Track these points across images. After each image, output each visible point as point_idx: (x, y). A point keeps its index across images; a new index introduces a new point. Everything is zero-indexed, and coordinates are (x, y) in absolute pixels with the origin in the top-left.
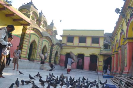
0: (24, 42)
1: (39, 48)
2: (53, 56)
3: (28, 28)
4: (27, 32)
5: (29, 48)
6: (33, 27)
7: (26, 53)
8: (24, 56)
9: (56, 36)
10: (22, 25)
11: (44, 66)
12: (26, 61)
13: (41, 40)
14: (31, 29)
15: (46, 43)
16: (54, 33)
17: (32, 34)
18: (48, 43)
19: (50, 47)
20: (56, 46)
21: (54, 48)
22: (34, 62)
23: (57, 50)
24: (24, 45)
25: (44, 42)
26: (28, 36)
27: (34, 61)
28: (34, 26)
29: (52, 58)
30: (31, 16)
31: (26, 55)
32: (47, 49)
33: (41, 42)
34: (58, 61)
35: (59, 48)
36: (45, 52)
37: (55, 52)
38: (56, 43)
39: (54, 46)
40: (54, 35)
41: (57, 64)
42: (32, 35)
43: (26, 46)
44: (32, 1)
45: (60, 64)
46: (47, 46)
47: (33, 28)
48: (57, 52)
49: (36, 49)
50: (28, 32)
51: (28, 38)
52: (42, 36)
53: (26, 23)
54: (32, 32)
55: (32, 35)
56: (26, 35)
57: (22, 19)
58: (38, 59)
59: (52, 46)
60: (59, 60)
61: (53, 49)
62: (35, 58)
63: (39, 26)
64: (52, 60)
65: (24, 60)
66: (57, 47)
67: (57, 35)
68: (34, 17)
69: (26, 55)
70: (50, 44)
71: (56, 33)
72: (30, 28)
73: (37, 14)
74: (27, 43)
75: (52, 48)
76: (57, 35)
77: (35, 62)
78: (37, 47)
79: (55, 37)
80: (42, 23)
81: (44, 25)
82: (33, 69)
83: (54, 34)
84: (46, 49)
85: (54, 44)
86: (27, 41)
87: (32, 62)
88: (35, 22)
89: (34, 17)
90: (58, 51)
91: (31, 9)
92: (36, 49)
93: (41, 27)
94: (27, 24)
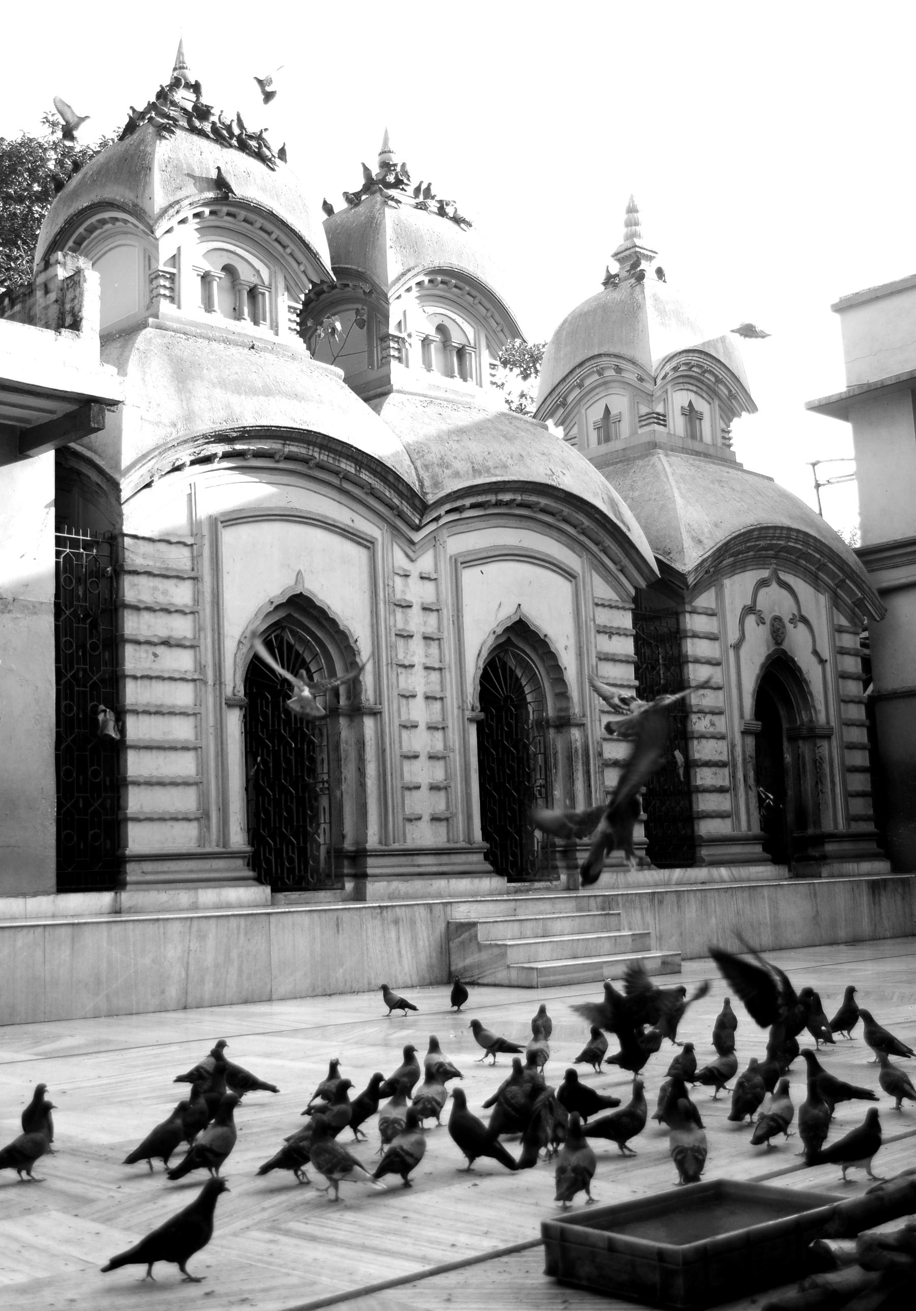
0: (134, 659)
1: (417, 681)
2: (704, 750)
3: (125, 462)
5: (234, 721)
6: (206, 426)
7: (203, 799)
8: (183, 837)
9: (742, 429)
11: (481, 932)
12: (208, 896)
13: (426, 563)
14: (185, 455)
15: (515, 585)
16: (680, 398)
17: (235, 519)
18: (568, 574)
19: (625, 620)
20: (739, 587)
21: (695, 623)
22: (359, 895)
23: (777, 632)
24: (134, 694)
25: (469, 576)
26: (180, 558)
27: (361, 876)
28: (234, 399)
29: (704, 777)
30: (206, 278)
31: (202, 817)
32: (568, 661)
33: (417, 592)
34: (841, 803)
35: (815, 603)
36: (542, 724)
37: (749, 683)
38: (721, 536)
39: (706, 600)
40: (677, 424)
41: (830, 848)
42: (228, 536)
43: (183, 695)
44: (180, 66)
45: (883, 845)
46: (556, 623)
47: (221, 438)
48: (780, 679)
49: (357, 711)
50: (148, 512)
51: (181, 594)
52: (423, 508)
54: (231, 489)
55: (228, 536)
56: (135, 556)
58: (425, 835)
59: (660, 603)
60: (860, 782)
61: (694, 648)
62: (372, 840)
64: (706, 803)
65: (184, 897)
66: (774, 600)
67: (752, 407)
68: (254, 267)
69: (202, 817)
70: (602, 590)
71: (710, 379)
72: (163, 448)
73: (271, 216)
74: (182, 661)
75: (677, 636)
76: (752, 407)
77: (373, 888)
78: (368, 679)
79: (721, 455)
80: (410, 314)
81: (464, 330)
82: (294, 996)
83: (691, 413)
84: (556, 670)
85: (689, 560)
86: (181, 627)
87: (325, 901)
88: (299, 344)
89: (246, 276)
90: (799, 644)
91: (157, 176)
92: (357, 711)
94: (69, 416)
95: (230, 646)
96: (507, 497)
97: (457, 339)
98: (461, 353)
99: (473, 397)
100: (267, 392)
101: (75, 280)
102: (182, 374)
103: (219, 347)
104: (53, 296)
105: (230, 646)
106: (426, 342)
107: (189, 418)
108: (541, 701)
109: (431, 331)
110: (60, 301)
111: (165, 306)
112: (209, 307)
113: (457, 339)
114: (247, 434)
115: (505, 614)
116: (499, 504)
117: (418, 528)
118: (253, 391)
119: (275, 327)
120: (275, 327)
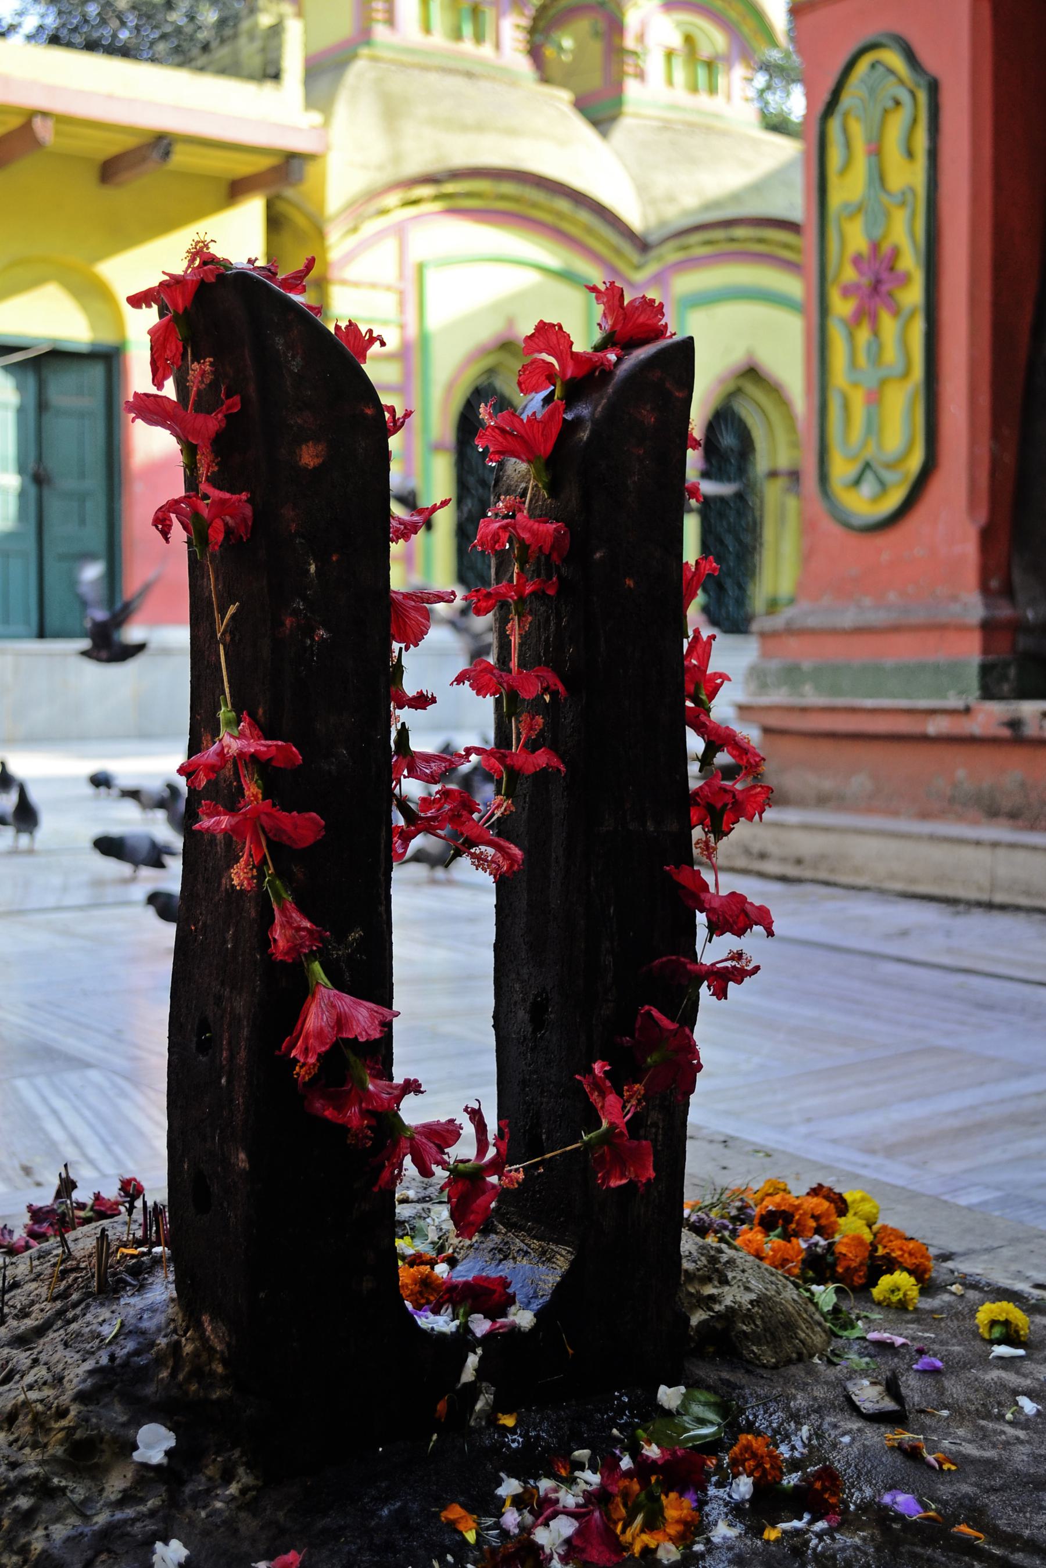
4: (349, 257)
6: (414, 167)
10: (236, 190)
53: (264, 163)
57: (161, 144)
63: (600, 110)
88: (523, 65)
93: (652, 92)
95: (437, 393)
96: (740, 232)
97: (705, 50)
98: (710, 65)
99: (717, 116)
100: (480, 128)
101: (276, 30)
102: (392, 112)
103: (433, 77)
104: (258, 44)
105: (437, 393)
106: (670, 55)
107: (396, 158)
108: (773, 451)
109: (676, 41)
110: (263, 50)
111: (380, 32)
112: (427, 29)
113: (705, 50)
114: (457, 175)
115: (736, 358)
116: (732, 240)
117: (638, 267)
118: (464, 128)
119: (498, 46)
120: (498, 46)
